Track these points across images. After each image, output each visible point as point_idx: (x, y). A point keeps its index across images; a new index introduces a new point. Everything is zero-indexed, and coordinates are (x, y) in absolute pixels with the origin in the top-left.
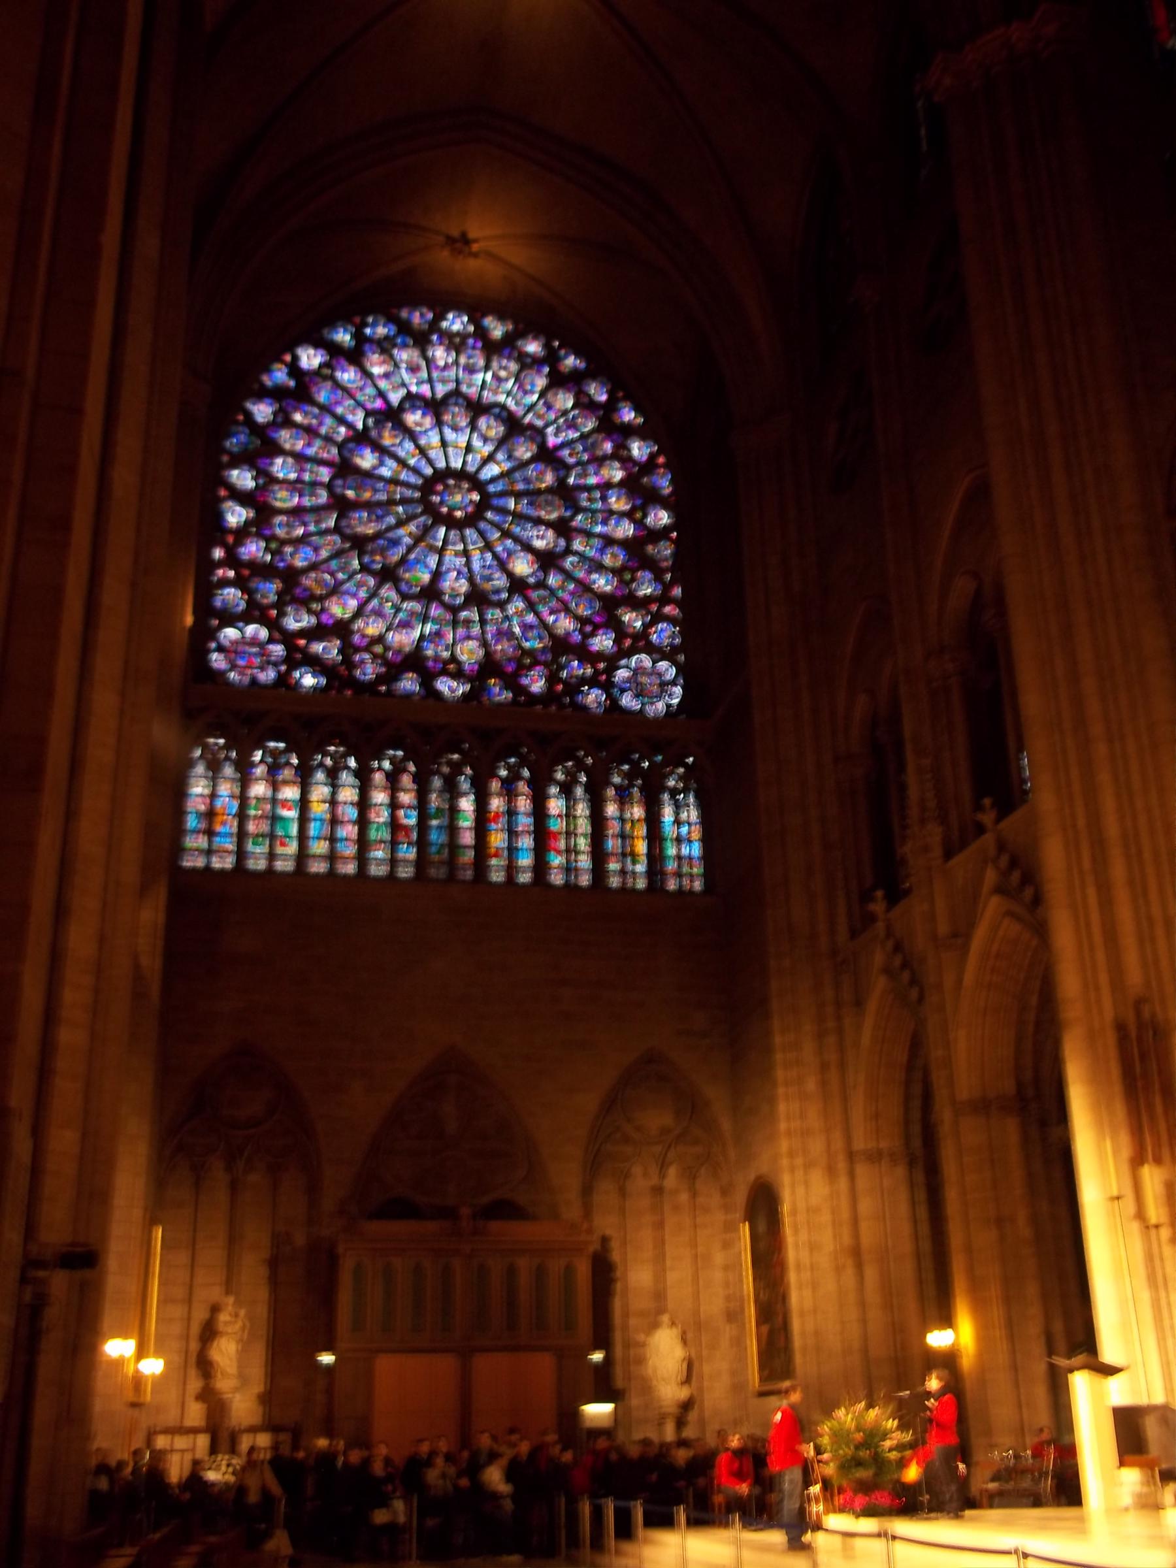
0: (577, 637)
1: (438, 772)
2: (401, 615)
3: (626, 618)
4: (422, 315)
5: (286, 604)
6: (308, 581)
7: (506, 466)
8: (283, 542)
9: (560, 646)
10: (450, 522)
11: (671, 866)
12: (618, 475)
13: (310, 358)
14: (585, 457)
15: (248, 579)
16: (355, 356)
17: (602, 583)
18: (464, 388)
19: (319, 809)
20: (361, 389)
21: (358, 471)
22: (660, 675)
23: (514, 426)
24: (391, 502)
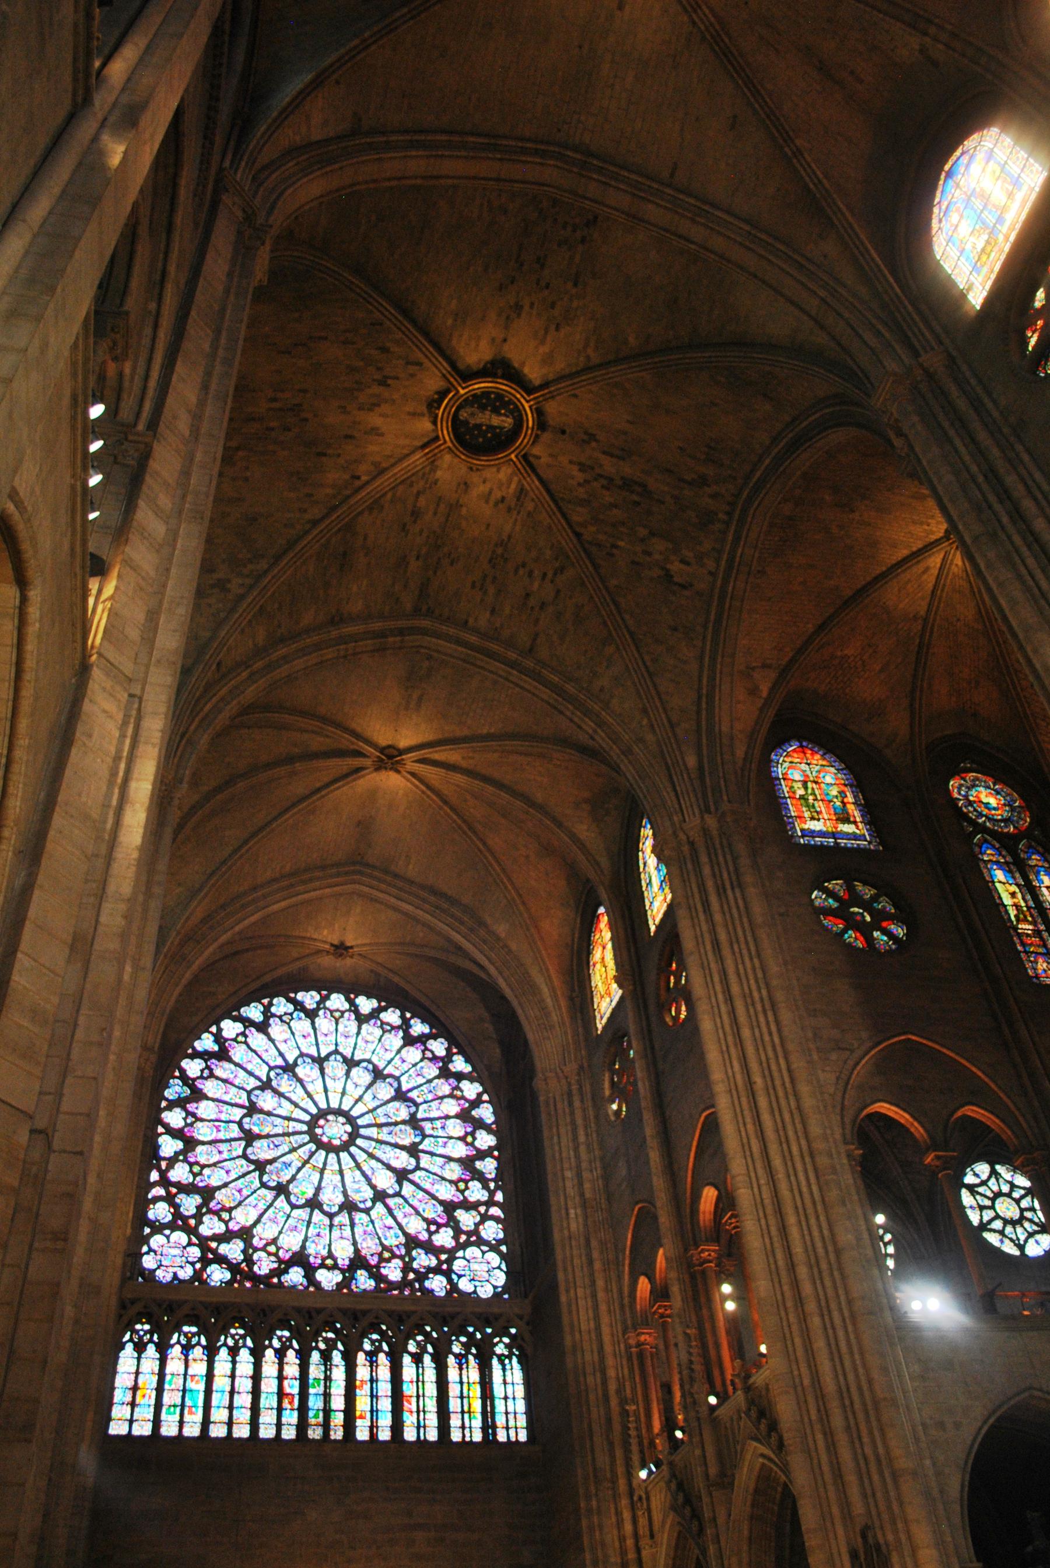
0: (424, 1236)
1: (317, 1348)
2: (290, 1221)
4: (312, 997)
6: (222, 1197)
7: (372, 1105)
8: (203, 1167)
9: (412, 1242)
10: (329, 1148)
11: (500, 1420)
13: (230, 1028)
14: (430, 1097)
15: (176, 1195)
16: (263, 1027)
18: (341, 1049)
19: (221, 1383)
21: (261, 1111)
23: (378, 1075)
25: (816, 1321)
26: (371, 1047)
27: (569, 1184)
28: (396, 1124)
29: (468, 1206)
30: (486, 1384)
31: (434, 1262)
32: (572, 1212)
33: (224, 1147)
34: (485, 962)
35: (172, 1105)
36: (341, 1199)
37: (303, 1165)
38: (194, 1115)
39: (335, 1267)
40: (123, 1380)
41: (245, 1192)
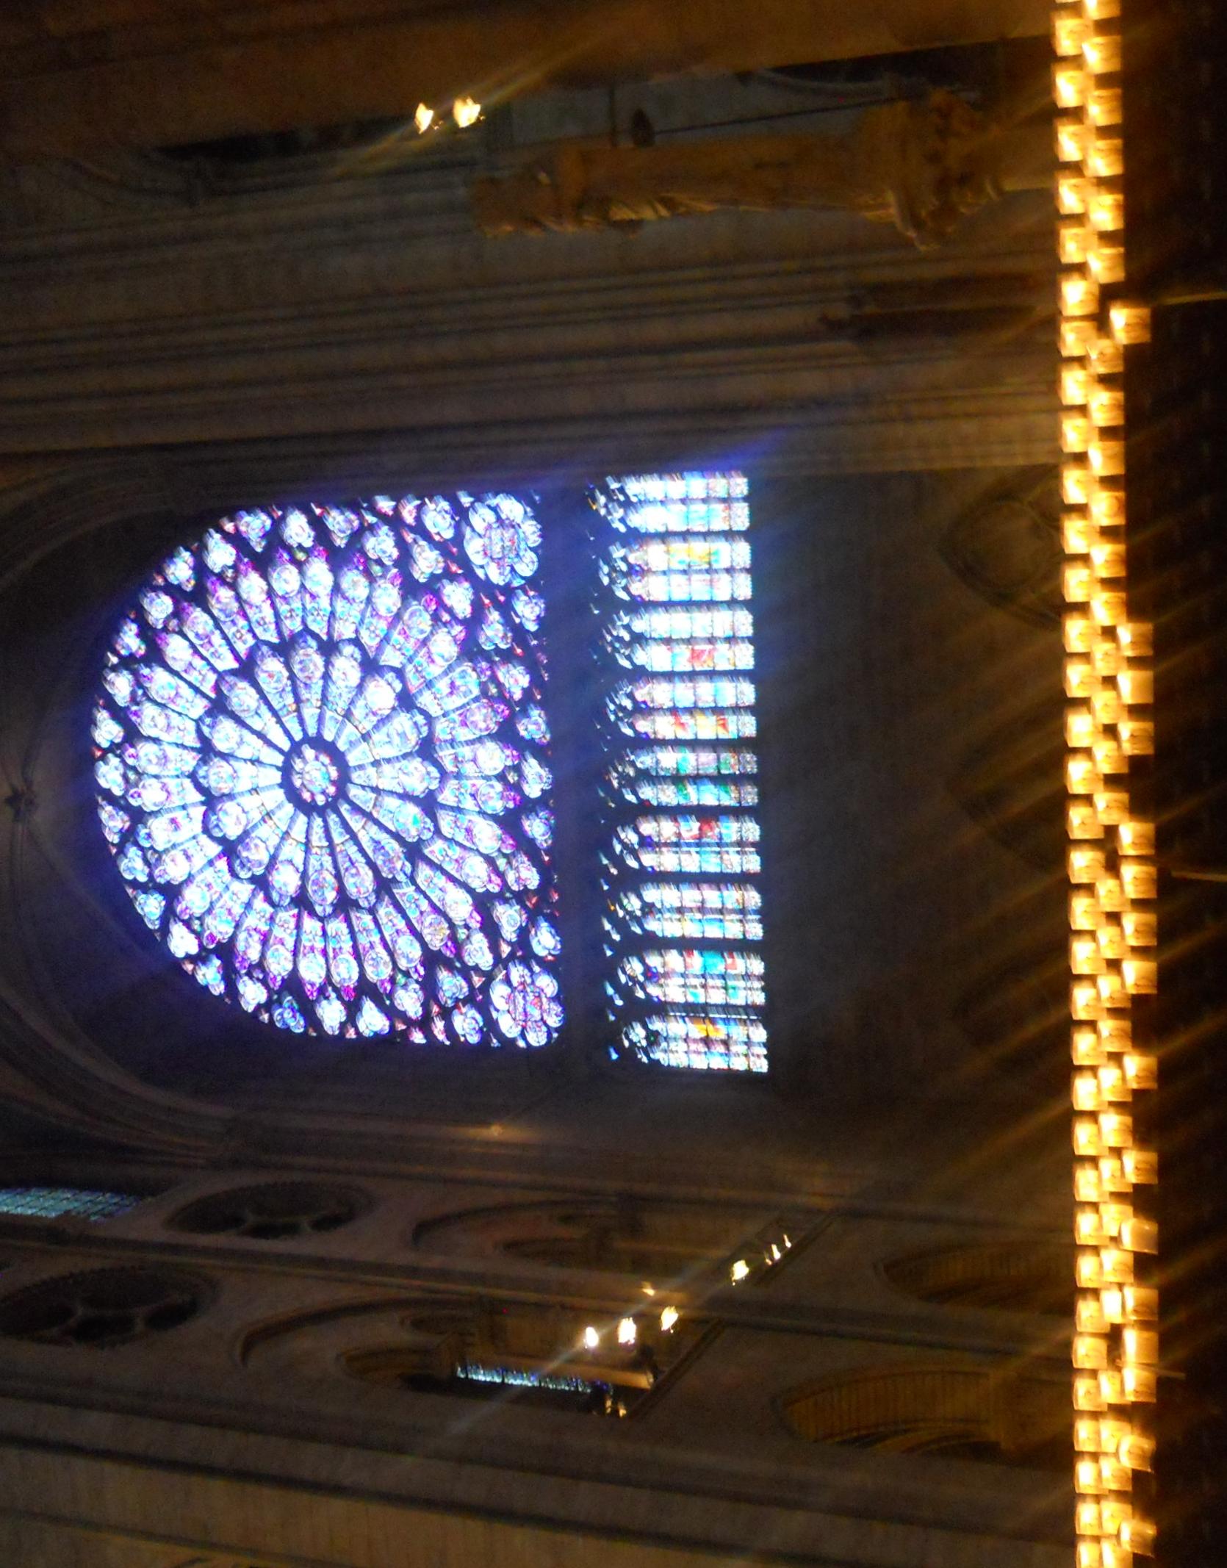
2: (460, 837)
3: (428, 571)
4: (111, 817)
5: (463, 963)
6: (436, 940)
8: (395, 966)
9: (470, 650)
10: (342, 782)
13: (182, 943)
14: (242, 622)
16: (171, 892)
17: (388, 597)
18: (189, 767)
19: (690, 928)
20: (209, 886)
21: (303, 888)
22: (489, 527)
23: (219, 707)
28: (292, 677)
30: (665, 536)
31: (494, 616)
35: (313, 1020)
39: (517, 769)
40: (700, 1063)
41: (424, 905)
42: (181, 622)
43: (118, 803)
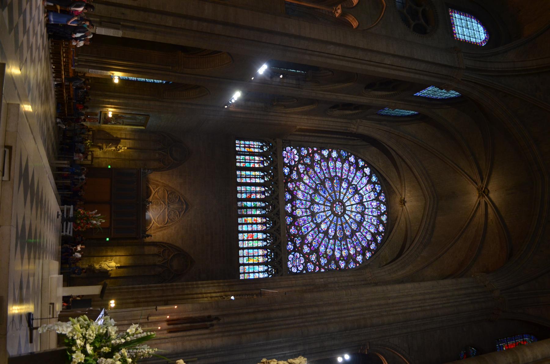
2: (306, 195)
8: (320, 165)
9: (304, 237)
12: (352, 253)
13: (367, 171)
14: (355, 243)
17: (322, 249)
18: (367, 210)
19: (253, 173)
23: (360, 224)
24: (335, 192)
25: (297, 312)
26: (369, 221)
27: (332, 279)
28: (343, 231)
29: (318, 258)
32: (322, 280)
33: (327, 171)
34: (410, 249)
35: (338, 153)
36: (316, 211)
37: (325, 198)
38: (337, 160)
39: (293, 211)
42: (368, 243)
43: (381, 202)
